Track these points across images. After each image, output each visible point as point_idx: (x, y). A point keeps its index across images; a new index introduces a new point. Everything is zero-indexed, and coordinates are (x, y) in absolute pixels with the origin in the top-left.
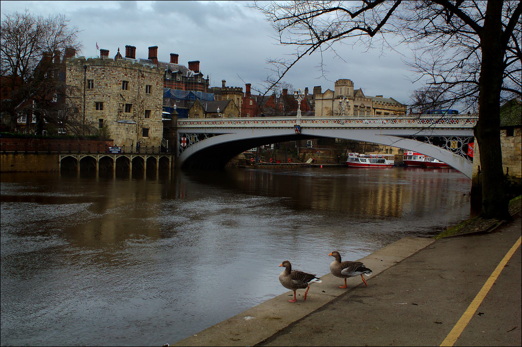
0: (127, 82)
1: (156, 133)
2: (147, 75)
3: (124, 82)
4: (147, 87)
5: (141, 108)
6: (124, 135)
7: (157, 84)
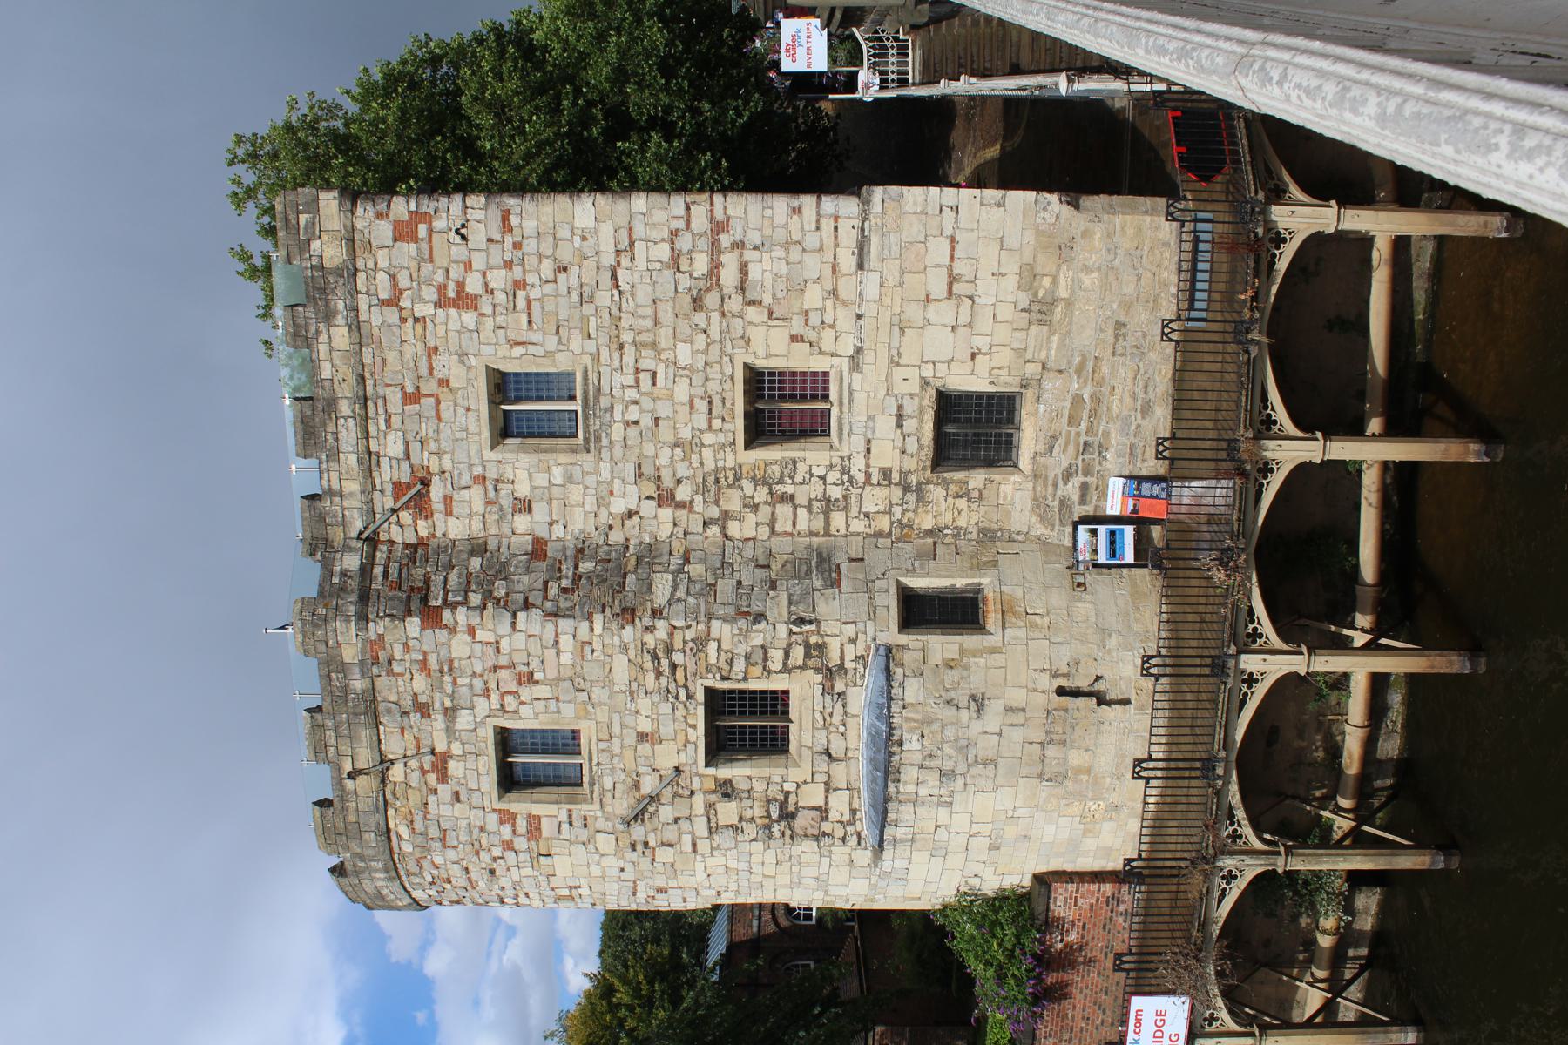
0: (506, 742)
1: (986, 292)
2: (393, 446)
3: (510, 780)
4: (505, 429)
5: (732, 501)
6: (1004, 799)
7: (465, 300)
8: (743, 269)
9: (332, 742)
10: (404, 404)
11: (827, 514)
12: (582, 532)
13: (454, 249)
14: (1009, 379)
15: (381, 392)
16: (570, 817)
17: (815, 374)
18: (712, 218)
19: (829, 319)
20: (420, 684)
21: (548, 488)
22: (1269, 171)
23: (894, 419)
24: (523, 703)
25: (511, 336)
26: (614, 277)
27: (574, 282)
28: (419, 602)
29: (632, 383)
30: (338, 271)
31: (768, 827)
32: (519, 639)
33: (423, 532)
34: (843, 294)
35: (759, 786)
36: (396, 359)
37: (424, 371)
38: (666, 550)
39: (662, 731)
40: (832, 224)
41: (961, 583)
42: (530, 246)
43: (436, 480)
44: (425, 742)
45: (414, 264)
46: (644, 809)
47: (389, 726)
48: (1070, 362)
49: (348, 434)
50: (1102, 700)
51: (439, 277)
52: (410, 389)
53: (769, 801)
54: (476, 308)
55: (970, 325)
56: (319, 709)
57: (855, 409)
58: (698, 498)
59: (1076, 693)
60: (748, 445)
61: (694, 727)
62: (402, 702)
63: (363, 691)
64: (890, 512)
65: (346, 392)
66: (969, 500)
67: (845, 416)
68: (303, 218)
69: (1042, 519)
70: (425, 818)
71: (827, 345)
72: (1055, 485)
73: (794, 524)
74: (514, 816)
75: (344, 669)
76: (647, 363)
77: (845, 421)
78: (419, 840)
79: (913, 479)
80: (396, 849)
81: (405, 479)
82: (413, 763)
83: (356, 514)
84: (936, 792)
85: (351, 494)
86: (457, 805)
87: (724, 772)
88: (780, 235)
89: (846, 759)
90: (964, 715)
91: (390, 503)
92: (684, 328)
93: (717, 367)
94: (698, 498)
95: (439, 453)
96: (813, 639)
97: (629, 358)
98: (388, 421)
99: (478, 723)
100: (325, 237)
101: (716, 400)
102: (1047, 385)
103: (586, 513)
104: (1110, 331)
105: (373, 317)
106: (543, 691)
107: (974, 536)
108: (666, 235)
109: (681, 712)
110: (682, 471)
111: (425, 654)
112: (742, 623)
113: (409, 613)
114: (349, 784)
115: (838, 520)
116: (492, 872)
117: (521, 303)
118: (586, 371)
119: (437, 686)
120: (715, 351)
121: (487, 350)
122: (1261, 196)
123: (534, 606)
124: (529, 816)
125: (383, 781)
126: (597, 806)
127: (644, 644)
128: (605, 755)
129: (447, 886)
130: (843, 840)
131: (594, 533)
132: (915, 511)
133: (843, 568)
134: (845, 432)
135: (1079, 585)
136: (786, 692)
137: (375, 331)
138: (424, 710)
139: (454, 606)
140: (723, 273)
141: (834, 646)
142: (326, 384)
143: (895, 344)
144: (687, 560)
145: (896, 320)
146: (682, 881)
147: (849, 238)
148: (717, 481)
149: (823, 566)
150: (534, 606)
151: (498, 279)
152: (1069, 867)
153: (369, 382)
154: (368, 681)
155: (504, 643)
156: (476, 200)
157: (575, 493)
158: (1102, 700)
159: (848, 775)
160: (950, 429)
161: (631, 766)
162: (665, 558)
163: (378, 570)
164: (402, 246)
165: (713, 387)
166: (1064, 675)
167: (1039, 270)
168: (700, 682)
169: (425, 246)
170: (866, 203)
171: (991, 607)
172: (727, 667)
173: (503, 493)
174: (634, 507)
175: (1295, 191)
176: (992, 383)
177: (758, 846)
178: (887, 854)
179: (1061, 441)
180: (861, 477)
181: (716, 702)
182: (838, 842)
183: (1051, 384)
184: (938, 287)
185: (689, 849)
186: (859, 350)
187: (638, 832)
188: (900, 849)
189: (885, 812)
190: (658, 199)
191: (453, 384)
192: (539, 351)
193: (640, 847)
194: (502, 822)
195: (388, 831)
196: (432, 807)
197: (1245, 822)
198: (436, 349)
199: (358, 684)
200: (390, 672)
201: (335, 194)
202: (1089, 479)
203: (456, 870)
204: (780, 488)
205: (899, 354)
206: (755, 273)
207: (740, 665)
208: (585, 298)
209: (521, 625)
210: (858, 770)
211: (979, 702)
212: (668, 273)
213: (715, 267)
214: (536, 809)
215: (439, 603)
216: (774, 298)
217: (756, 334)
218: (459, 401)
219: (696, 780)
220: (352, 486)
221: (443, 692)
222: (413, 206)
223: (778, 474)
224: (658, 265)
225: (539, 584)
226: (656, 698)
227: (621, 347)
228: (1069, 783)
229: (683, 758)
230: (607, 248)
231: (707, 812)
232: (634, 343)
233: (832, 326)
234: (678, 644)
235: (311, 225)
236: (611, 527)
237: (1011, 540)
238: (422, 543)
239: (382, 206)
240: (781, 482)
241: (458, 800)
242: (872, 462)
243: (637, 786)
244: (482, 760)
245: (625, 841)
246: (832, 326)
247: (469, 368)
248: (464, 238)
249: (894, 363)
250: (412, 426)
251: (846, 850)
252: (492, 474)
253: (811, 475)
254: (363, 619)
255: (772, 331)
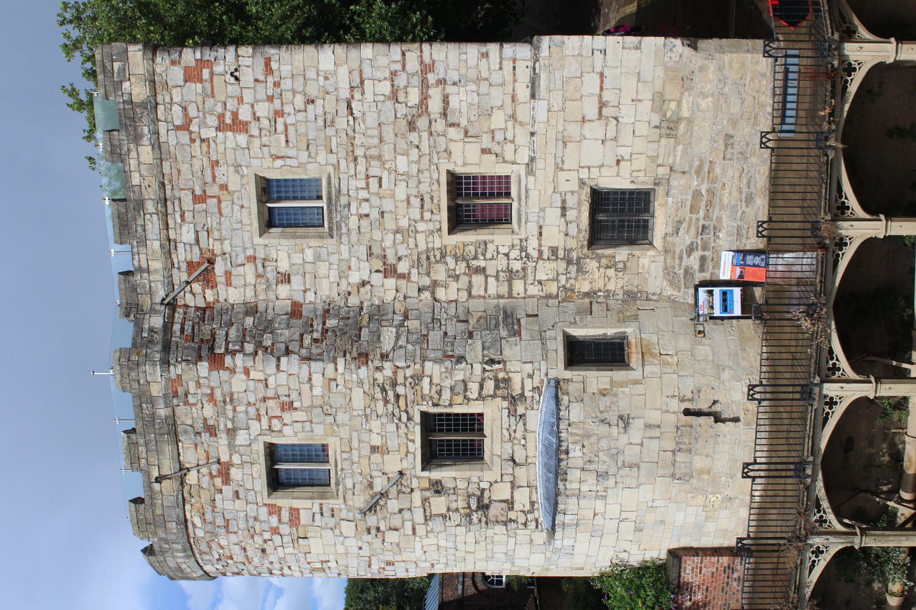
0: (273, 453)
1: (627, 114)
2: (187, 235)
3: (276, 482)
4: (270, 221)
5: (439, 273)
6: (645, 493)
7: (238, 126)
8: (446, 100)
9: (144, 455)
10: (194, 203)
11: (510, 282)
12: (328, 297)
13: (230, 88)
14: (645, 179)
15: (177, 194)
16: (321, 509)
17: (500, 177)
18: (422, 62)
19: (510, 136)
20: (209, 411)
21: (303, 265)
22: (842, 16)
23: (559, 210)
24: (285, 425)
25: (274, 152)
26: (349, 107)
27: (320, 111)
28: (208, 351)
29: (364, 186)
30: (144, 105)
31: (469, 515)
32: (283, 377)
33: (210, 299)
34: (520, 118)
35: (462, 485)
36: (188, 170)
37: (209, 179)
38: (391, 310)
39: (389, 444)
40: (512, 65)
41: (611, 332)
42: (286, 84)
43: (219, 260)
44: (213, 454)
45: (200, 99)
46: (377, 503)
47: (186, 443)
48: (691, 166)
49: (153, 226)
50: (718, 419)
51: (219, 109)
52: (198, 192)
53: (469, 496)
54: (247, 132)
55: (615, 139)
56: (134, 430)
57: (530, 203)
58: (414, 271)
59: (698, 413)
60: (451, 231)
61: (413, 441)
62: (196, 425)
63: (166, 417)
64: (557, 280)
65: (151, 195)
66: (616, 270)
67: (523, 209)
68: (116, 65)
69: (671, 283)
70: (213, 511)
71: (509, 156)
72: (681, 258)
73: (486, 289)
74: (280, 509)
75: (152, 401)
76: (374, 171)
77: (523, 212)
78: (209, 528)
79: (574, 255)
80: (192, 535)
81: (196, 259)
82: (204, 470)
83: (160, 286)
84: (594, 488)
85: (156, 271)
86: (237, 501)
87: (436, 474)
88: (473, 74)
89: (526, 464)
90: (615, 430)
91: (185, 277)
92: (402, 145)
93: (427, 174)
94: (414, 271)
95: (221, 240)
96: (501, 375)
97: (361, 168)
98: (182, 216)
99: (252, 441)
100: (133, 79)
101: (427, 198)
102: (674, 183)
103: (331, 283)
104: (721, 142)
105: (170, 138)
106: (300, 416)
107: (620, 297)
108: (387, 75)
109: (403, 430)
110: (402, 251)
111: (212, 389)
112: (448, 364)
113: (200, 358)
114: (157, 486)
115: (518, 286)
116: (264, 551)
117: (280, 127)
118: (329, 178)
119: (221, 413)
120: (425, 161)
121: (255, 163)
122: (836, 36)
123: (293, 352)
124: (291, 509)
125: (182, 484)
126: (341, 501)
127: (375, 380)
128: (347, 462)
129: (230, 562)
130: (525, 524)
131: (337, 298)
132: (576, 279)
133: (523, 321)
134: (523, 221)
135: (700, 332)
136: (481, 415)
137: (172, 149)
138: (212, 431)
139: (233, 353)
140: (431, 103)
141: (516, 380)
142: (136, 189)
143: (560, 154)
144: (406, 317)
145: (560, 137)
146: (405, 556)
147: (524, 76)
148: (428, 258)
149: (508, 320)
150: (293, 352)
151: (263, 110)
152: (695, 544)
153: (168, 187)
154: (170, 409)
155: (271, 381)
156: (246, 51)
157: (323, 268)
158: (718, 419)
159: (528, 476)
160: (601, 217)
161: (366, 470)
162: (390, 316)
163: (177, 327)
164: (191, 86)
165: (424, 188)
166: (689, 400)
167: (667, 97)
168: (417, 407)
169: (208, 85)
170: (537, 48)
171: (633, 350)
172: (436, 396)
173: (269, 269)
174: (366, 279)
175: (863, 32)
176: (632, 182)
177: (462, 529)
178: (558, 535)
179: (685, 225)
180: (535, 254)
181: (430, 423)
182: (521, 526)
183: (677, 182)
184: (591, 110)
185: (410, 532)
186: (532, 159)
187: (372, 520)
188: (568, 531)
189: (556, 503)
190: (381, 48)
191: (230, 188)
192: (294, 162)
193: (373, 531)
194: (270, 514)
195: (186, 521)
196: (218, 503)
197: (829, 510)
198: (218, 162)
199: (162, 412)
200: (186, 403)
201: (140, 46)
202: (706, 253)
203: (236, 550)
204: (475, 263)
205: (563, 162)
206: (454, 102)
207: (447, 395)
208: (328, 123)
209: (283, 366)
210: (535, 472)
211: (625, 421)
212: (389, 104)
213: (424, 98)
214: (296, 504)
215: (222, 351)
216: (469, 121)
217: (456, 148)
218: (236, 201)
219: (415, 481)
220: (157, 265)
221: (226, 418)
222: (198, 56)
223: (473, 253)
224: (382, 98)
225: (297, 337)
226: (384, 420)
227: (355, 159)
228: (694, 481)
229: (405, 465)
230: (344, 85)
231: (423, 505)
232: (365, 156)
233: (513, 142)
234: (400, 380)
235: (122, 70)
236: (349, 293)
237: (648, 299)
238: (209, 307)
239: (175, 56)
240: (475, 258)
241: (238, 498)
242: (543, 242)
243: (371, 486)
244: (256, 468)
245: (362, 527)
246: (513, 142)
247: (242, 176)
248: (237, 79)
249: (559, 168)
250: (200, 219)
251: (527, 532)
252: (261, 255)
253: (498, 253)
254: (165, 363)
255: (467, 145)
